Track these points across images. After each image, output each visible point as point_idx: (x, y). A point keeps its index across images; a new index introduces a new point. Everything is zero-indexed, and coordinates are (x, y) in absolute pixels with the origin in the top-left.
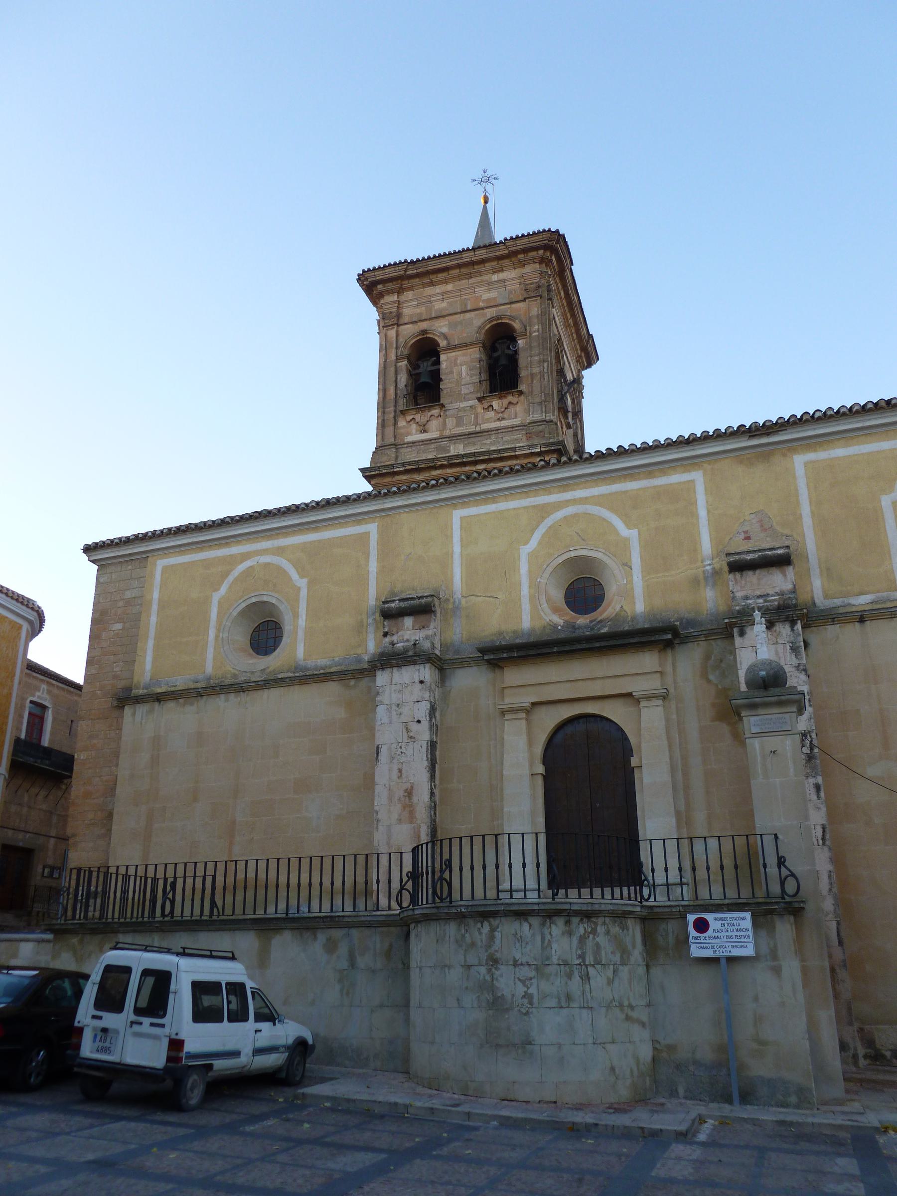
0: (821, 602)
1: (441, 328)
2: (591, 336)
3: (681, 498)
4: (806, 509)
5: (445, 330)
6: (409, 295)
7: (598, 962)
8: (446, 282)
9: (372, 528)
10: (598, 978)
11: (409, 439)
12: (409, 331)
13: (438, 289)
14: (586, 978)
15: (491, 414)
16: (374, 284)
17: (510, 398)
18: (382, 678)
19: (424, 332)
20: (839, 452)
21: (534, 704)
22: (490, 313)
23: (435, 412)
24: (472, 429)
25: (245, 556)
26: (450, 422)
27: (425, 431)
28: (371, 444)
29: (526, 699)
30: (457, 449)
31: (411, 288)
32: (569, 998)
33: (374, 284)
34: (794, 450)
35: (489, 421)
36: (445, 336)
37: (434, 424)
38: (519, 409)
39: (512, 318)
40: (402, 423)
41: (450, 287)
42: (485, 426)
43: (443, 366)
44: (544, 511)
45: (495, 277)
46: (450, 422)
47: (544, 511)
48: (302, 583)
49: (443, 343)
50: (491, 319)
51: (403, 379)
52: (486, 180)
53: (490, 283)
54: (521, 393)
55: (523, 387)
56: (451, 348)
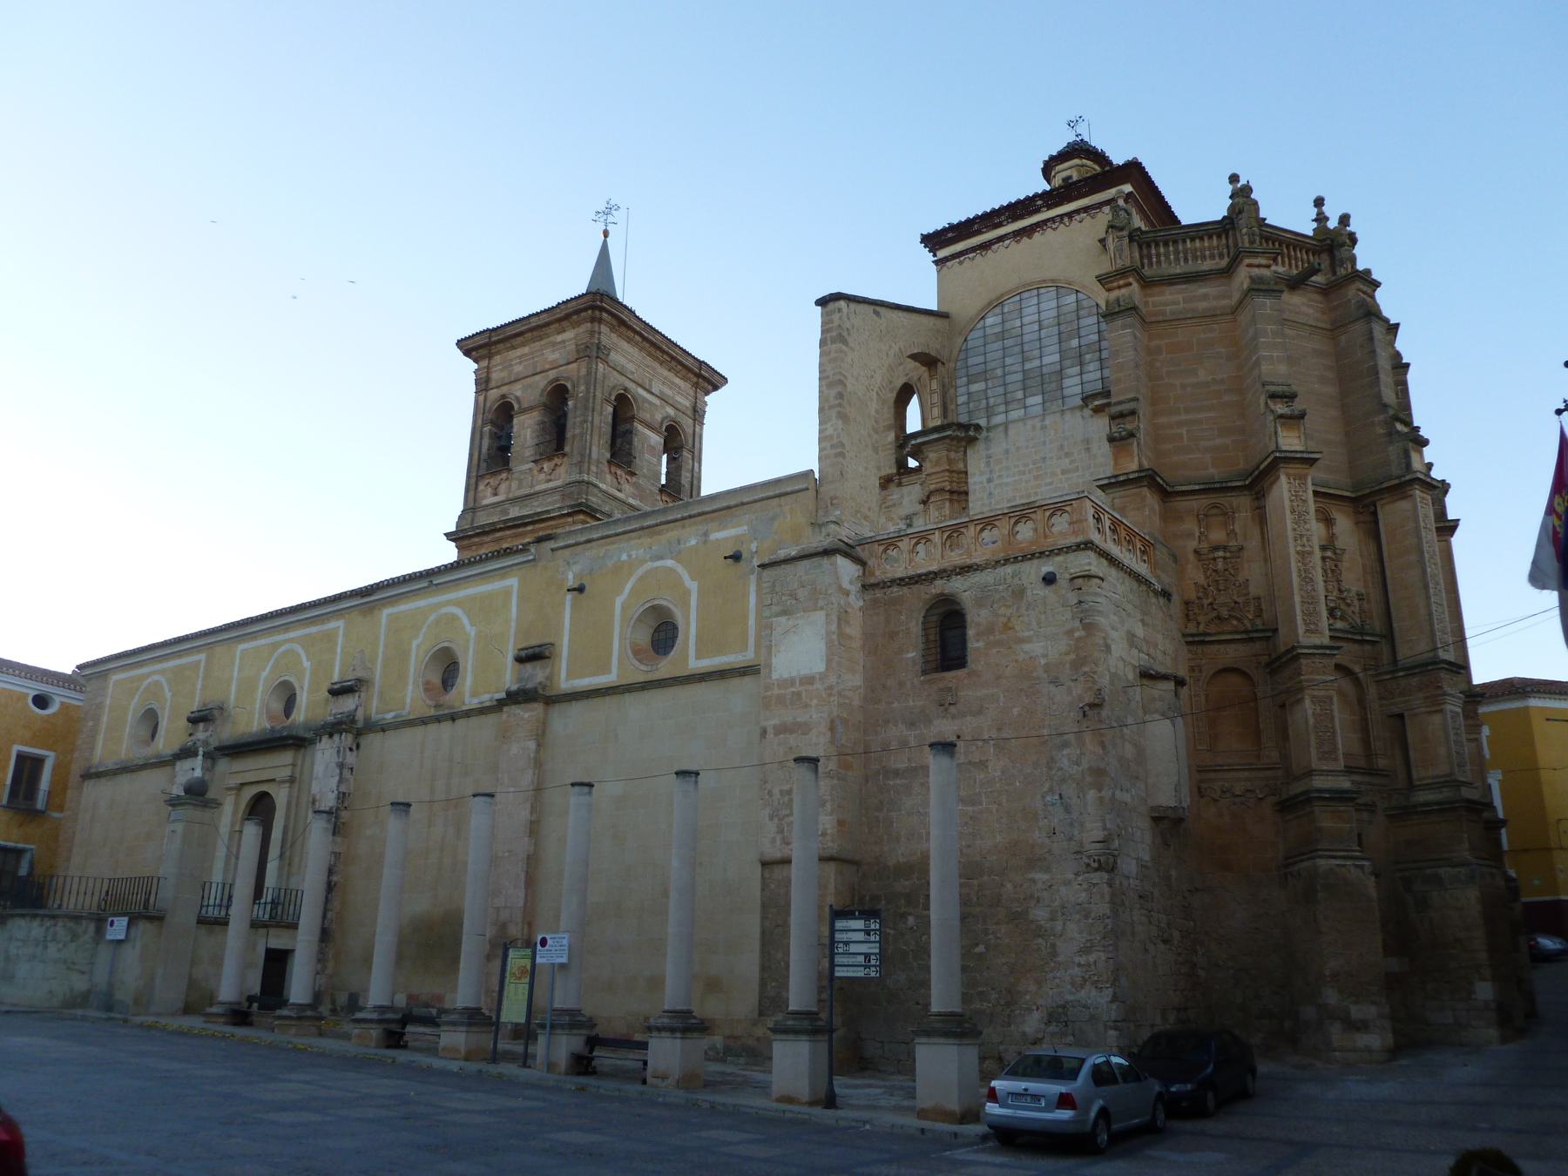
0: (374, 717)
1: (517, 390)
2: (702, 363)
3: (330, 637)
4: (381, 649)
5: (518, 393)
6: (497, 359)
7: (54, 940)
8: (523, 345)
9: (202, 656)
10: (52, 948)
11: (485, 502)
12: (494, 394)
13: (519, 352)
14: (46, 947)
15: (542, 476)
16: (473, 346)
17: (557, 461)
18: (179, 765)
19: (503, 396)
20: (403, 607)
21: (243, 784)
22: (552, 374)
23: (504, 475)
24: (527, 491)
25: (149, 675)
26: (514, 484)
27: (496, 494)
28: (456, 505)
29: (235, 781)
30: (515, 512)
31: (498, 353)
32: (34, 956)
33: (473, 346)
34: (384, 605)
35: (539, 483)
36: (517, 399)
37: (503, 487)
38: (561, 470)
39: (568, 379)
40: (481, 487)
41: (526, 350)
42: (538, 488)
43: (515, 429)
44: (275, 646)
45: (559, 338)
46: (514, 484)
47: (275, 646)
48: (168, 695)
49: (516, 406)
50: (551, 382)
51: (486, 443)
52: (609, 211)
53: (554, 344)
54: (564, 455)
55: (567, 449)
56: (523, 411)
